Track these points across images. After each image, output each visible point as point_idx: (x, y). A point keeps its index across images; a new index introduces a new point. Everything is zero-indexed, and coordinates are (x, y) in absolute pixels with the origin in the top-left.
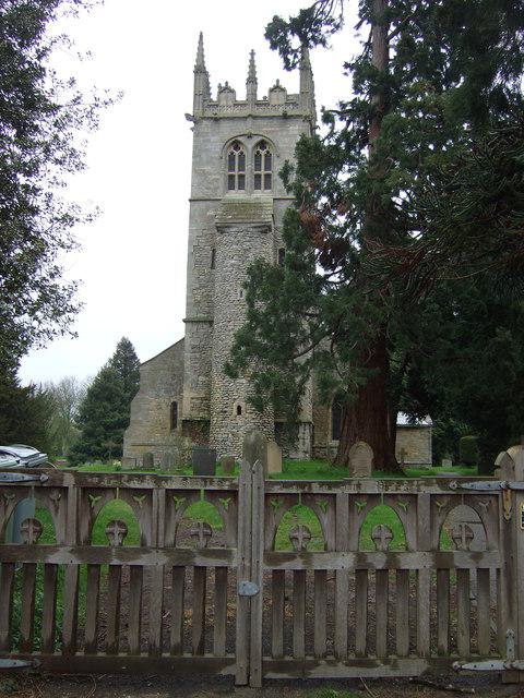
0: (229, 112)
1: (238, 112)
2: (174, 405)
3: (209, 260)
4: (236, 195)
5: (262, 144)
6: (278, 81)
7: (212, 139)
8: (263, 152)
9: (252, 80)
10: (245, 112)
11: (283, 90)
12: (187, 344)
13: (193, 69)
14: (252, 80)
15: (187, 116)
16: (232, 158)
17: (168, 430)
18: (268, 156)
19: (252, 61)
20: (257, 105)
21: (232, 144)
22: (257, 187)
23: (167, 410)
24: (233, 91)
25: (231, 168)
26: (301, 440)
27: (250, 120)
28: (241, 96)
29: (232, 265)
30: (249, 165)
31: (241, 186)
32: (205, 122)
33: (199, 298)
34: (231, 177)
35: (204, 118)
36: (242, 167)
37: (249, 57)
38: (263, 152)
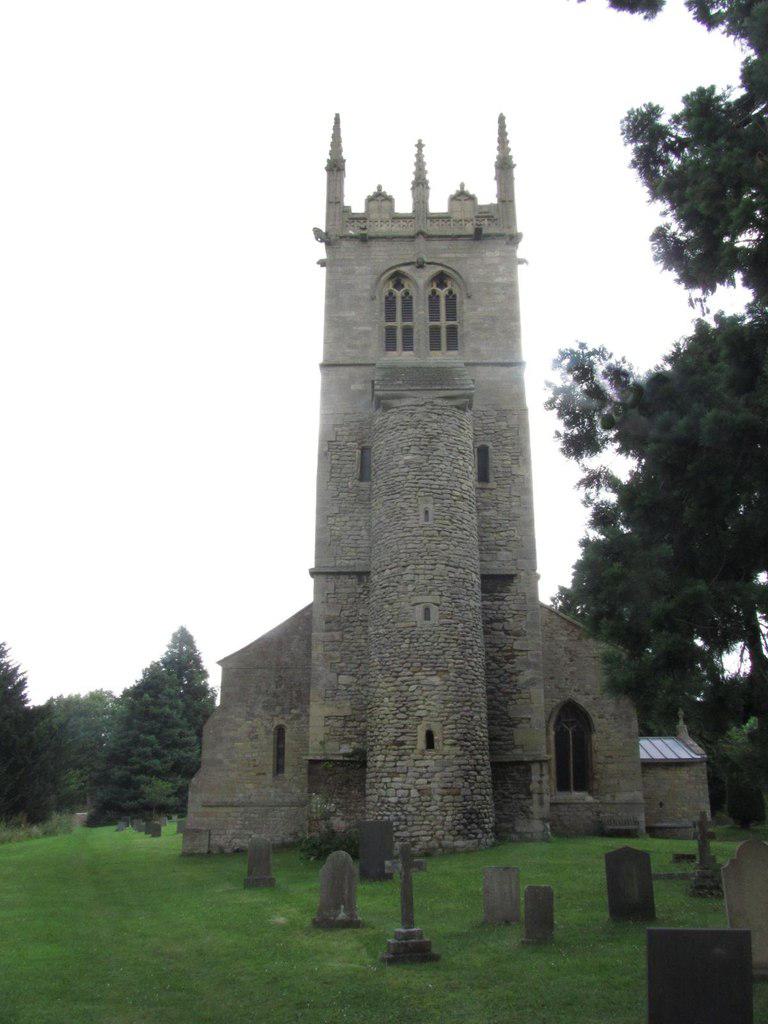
0: (384, 229)
1: (397, 229)
2: (280, 732)
3: (356, 467)
4: (402, 357)
5: (441, 279)
6: (462, 186)
8: (442, 293)
9: (420, 184)
10: (410, 230)
11: (472, 198)
12: (319, 622)
13: (326, 164)
14: (420, 184)
15: (317, 232)
16: (390, 301)
17: (270, 776)
18: (451, 299)
19: (419, 157)
20: (428, 218)
21: (391, 277)
22: (435, 344)
23: (267, 741)
24: (390, 199)
25: (390, 316)
26: (535, 797)
27: (421, 241)
28: (404, 205)
29: (408, 464)
30: (421, 310)
31: (408, 344)
32: (345, 243)
34: (390, 333)
36: (408, 314)
37: (415, 150)
38: (442, 293)
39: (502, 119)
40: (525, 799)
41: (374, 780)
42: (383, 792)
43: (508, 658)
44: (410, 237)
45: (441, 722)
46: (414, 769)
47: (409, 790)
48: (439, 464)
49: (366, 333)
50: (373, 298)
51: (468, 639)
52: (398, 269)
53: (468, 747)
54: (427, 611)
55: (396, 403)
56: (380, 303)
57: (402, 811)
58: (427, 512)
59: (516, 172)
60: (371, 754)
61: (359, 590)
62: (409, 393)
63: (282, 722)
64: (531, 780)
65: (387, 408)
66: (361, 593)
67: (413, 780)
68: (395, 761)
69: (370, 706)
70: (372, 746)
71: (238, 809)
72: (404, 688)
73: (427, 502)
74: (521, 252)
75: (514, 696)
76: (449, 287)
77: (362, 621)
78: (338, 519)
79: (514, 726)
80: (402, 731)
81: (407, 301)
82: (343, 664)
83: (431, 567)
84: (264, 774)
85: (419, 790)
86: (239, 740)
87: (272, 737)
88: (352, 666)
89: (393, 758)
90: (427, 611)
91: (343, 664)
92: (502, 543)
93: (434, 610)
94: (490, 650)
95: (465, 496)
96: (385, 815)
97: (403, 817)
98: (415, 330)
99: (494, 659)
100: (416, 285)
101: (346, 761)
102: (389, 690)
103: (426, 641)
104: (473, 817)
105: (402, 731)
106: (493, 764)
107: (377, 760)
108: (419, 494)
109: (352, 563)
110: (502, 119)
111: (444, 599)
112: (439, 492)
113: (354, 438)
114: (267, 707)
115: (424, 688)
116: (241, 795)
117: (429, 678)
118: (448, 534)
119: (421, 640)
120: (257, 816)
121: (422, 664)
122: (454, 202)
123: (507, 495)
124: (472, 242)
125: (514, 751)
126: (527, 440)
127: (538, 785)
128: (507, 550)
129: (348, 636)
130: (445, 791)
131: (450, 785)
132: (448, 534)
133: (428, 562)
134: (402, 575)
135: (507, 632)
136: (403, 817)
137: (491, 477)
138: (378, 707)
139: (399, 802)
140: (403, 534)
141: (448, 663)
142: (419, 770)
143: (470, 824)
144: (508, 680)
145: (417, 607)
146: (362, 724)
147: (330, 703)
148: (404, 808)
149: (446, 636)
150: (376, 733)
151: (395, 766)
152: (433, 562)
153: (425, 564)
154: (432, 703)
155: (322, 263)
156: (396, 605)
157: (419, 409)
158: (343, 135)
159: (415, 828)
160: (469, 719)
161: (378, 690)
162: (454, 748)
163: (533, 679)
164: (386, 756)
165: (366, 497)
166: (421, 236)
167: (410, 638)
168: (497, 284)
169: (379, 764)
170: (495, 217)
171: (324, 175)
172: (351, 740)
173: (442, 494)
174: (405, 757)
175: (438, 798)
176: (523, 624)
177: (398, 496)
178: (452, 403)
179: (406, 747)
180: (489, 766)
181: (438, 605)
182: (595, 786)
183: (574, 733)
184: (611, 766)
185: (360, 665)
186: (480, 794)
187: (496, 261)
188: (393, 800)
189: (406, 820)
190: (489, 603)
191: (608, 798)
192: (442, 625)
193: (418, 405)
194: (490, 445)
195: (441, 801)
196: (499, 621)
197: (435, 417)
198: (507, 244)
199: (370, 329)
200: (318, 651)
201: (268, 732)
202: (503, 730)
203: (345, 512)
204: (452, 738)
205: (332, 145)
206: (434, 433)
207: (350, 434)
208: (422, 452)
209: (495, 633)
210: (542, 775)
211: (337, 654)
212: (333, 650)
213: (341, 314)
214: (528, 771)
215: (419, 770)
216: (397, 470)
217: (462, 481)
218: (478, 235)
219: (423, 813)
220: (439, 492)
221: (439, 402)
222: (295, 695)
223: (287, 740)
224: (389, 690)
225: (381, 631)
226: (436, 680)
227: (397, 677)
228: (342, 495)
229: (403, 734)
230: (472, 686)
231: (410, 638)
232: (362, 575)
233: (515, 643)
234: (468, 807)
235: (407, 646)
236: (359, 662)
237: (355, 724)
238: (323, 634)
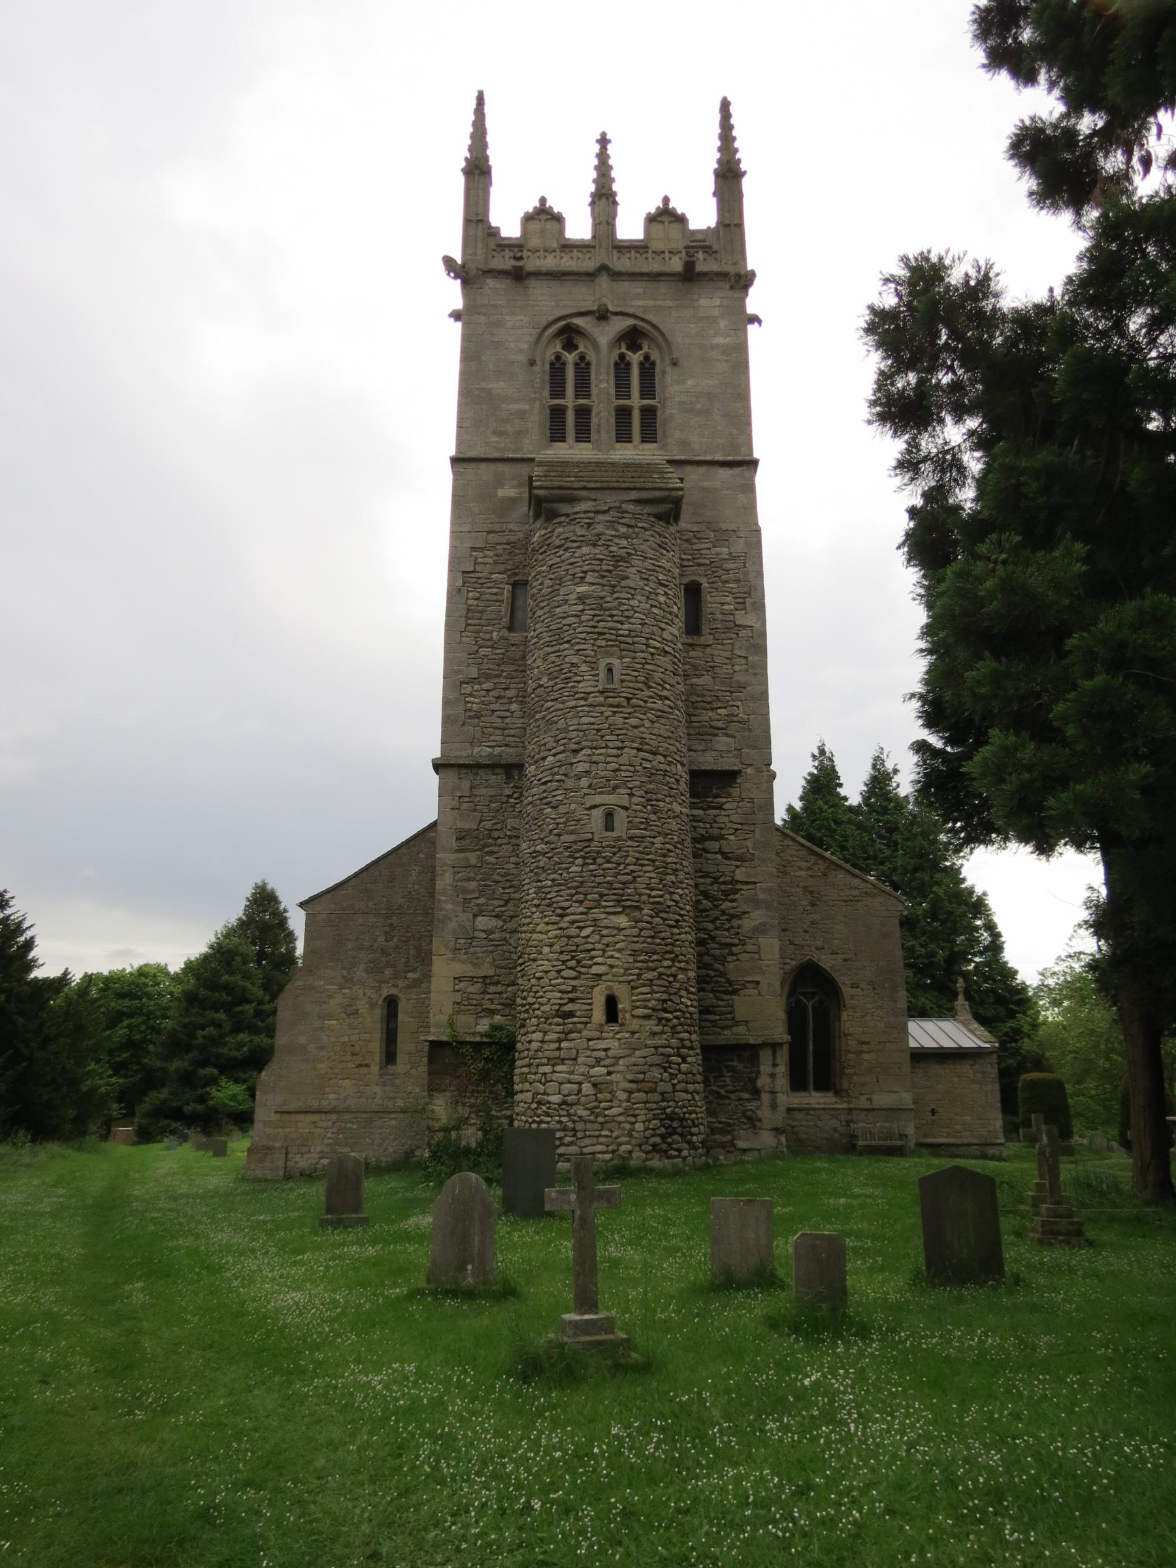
0: (550, 262)
1: (567, 263)
2: (392, 1004)
3: (504, 608)
4: (570, 451)
5: (632, 338)
7: (511, 320)
8: (635, 358)
10: (589, 265)
11: (681, 220)
12: (446, 838)
13: (463, 164)
15: (448, 262)
16: (557, 369)
17: (375, 1068)
18: (648, 369)
20: (615, 247)
22: (623, 435)
23: (373, 1020)
24: (558, 219)
25: (557, 388)
26: (765, 1097)
27: (604, 281)
28: (579, 227)
29: (582, 598)
30: (603, 383)
31: (583, 434)
32: (491, 282)
33: (475, 704)
34: (557, 414)
35: (488, 272)
37: (596, 148)
38: (635, 358)
39: (725, 106)
40: (748, 1100)
41: (526, 1070)
42: (541, 1088)
43: (726, 893)
44: (588, 274)
45: (629, 982)
46: (589, 1053)
47: (580, 1083)
48: (628, 599)
49: (522, 414)
50: (532, 363)
51: (669, 860)
52: (569, 321)
53: (668, 1020)
54: (609, 816)
55: (565, 508)
56: (542, 369)
57: (569, 1115)
58: (610, 670)
59: (746, 183)
60: (523, 1031)
61: (507, 792)
62: (584, 493)
63: (394, 991)
64: (759, 1072)
65: (552, 516)
66: (509, 796)
67: (583, 1069)
68: (559, 1041)
69: (521, 961)
70: (525, 1020)
71: (329, 1116)
72: (573, 931)
73: (611, 655)
74: (754, 303)
75: (735, 950)
76: (645, 349)
77: (510, 837)
78: (476, 687)
79: (735, 992)
80: (570, 995)
81: (583, 367)
82: (482, 901)
83: (615, 752)
84: (367, 1066)
85: (594, 1085)
86: (329, 1017)
87: (378, 1012)
88: (495, 902)
89: (554, 1036)
90: (609, 816)
91: (482, 901)
92: (719, 724)
93: (620, 817)
94: (702, 880)
95: (667, 649)
96: (542, 1122)
97: (570, 1125)
98: (594, 413)
99: (705, 894)
100: (595, 345)
101: (485, 1043)
102: (551, 934)
103: (608, 862)
104: (675, 1124)
105: (570, 995)
106: (703, 1048)
107: (531, 1040)
108: (599, 643)
109: (497, 750)
110: (725, 106)
111: (635, 800)
112: (630, 640)
113: (502, 568)
114: (374, 969)
115: (604, 932)
116: (331, 1096)
117: (611, 917)
118: (642, 703)
119: (599, 860)
120: (355, 1126)
121: (601, 895)
122: (655, 226)
123: (728, 654)
124: (680, 284)
125: (734, 1030)
126: (760, 574)
127: (768, 1080)
128: (728, 735)
129: (491, 859)
130: (634, 1086)
131: (641, 1076)
132: (642, 703)
133: (610, 744)
134: (572, 764)
135: (725, 855)
136: (570, 1125)
137: (705, 629)
138: (534, 960)
139: (564, 1103)
140: (573, 703)
141: (640, 895)
142: (595, 1054)
143: (670, 1135)
144: (727, 926)
145: (594, 812)
146: (510, 989)
147: (465, 957)
148: (572, 1111)
149: (638, 855)
150: (530, 1000)
151: (559, 1049)
152: (620, 745)
153: (607, 747)
154: (618, 955)
155: (456, 316)
156: (562, 809)
157: (600, 517)
158: (489, 124)
159: (587, 1141)
160: (671, 979)
161: (535, 936)
162: (645, 1022)
163: (763, 924)
164: (545, 1033)
165: (519, 654)
166: (604, 273)
167: (584, 858)
168: (718, 346)
169: (534, 1046)
170: (715, 248)
171: (460, 181)
172: (493, 1012)
173: (634, 643)
174: (574, 1035)
175: (623, 1096)
176: (749, 844)
177: (566, 646)
178: (648, 509)
179: (575, 1019)
180: (698, 1051)
181: (626, 808)
182: (845, 1085)
183: (814, 1009)
184: (866, 1056)
185: (507, 902)
186: (686, 1091)
187: (716, 312)
188: (555, 1099)
189: (574, 1129)
190: (701, 812)
191: (863, 1103)
192: (631, 838)
193: (597, 512)
194: (703, 581)
195: (628, 1100)
196: (713, 838)
197: (623, 530)
198: (732, 288)
199: (527, 407)
200: (445, 880)
201: (373, 1006)
202: (718, 999)
203: (488, 677)
204: (645, 1007)
205: (473, 136)
206: (622, 552)
207: (495, 562)
208: (604, 581)
209: (709, 856)
210: (775, 1065)
211: (473, 884)
212: (469, 880)
213: (483, 385)
214: (754, 1060)
215: (595, 1054)
216: (565, 608)
217: (663, 626)
218: (689, 276)
219: (600, 1119)
220: (630, 640)
221: (630, 507)
222: (413, 952)
223: (402, 1017)
224: (551, 934)
225: (539, 848)
226: (622, 921)
227: (562, 916)
228: (483, 651)
229: (571, 1000)
230: (676, 930)
231: (584, 858)
232: (512, 770)
233: (738, 871)
234: (668, 1110)
235: (579, 869)
236: (506, 897)
237: (499, 988)
238: (453, 856)
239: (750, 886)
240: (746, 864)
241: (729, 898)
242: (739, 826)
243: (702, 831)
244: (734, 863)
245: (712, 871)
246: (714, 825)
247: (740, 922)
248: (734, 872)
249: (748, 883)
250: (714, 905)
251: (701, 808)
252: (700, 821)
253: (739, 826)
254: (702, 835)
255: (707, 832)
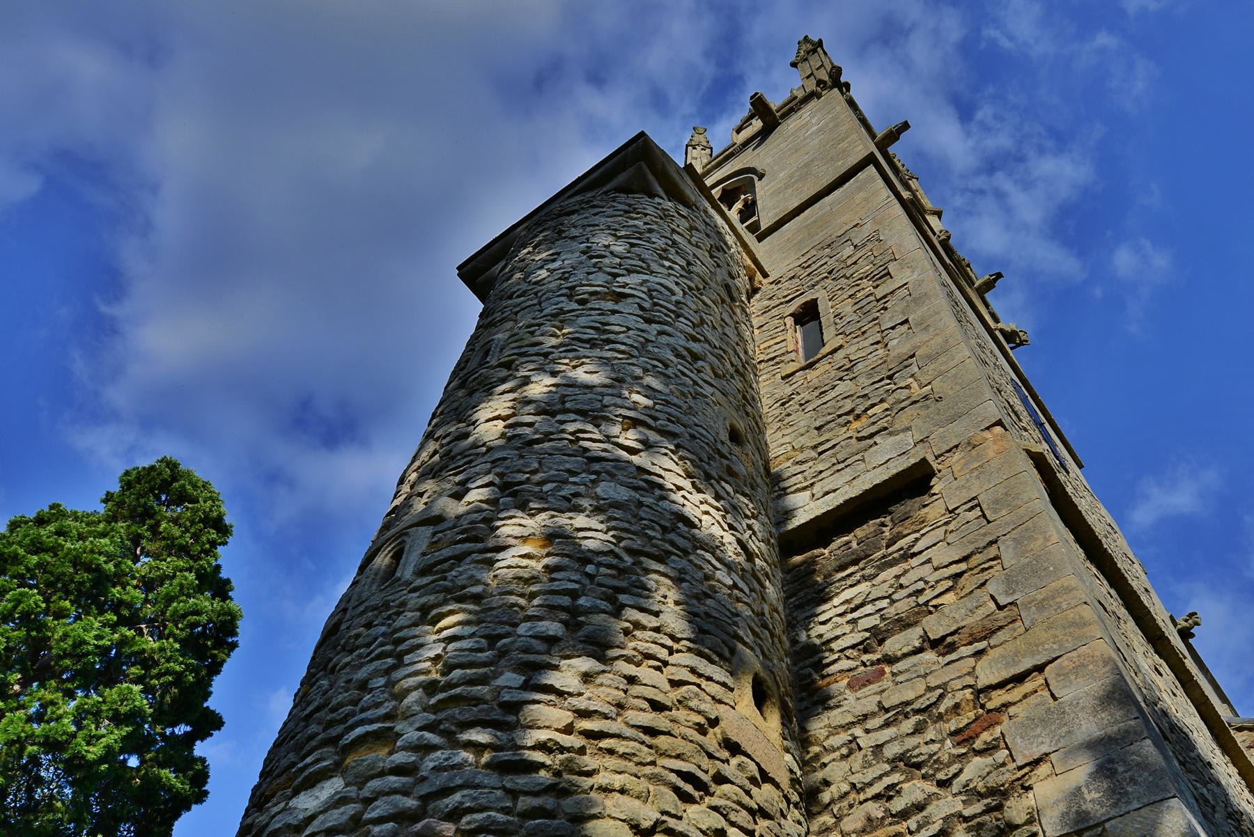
43: (962, 736)
196: (903, 624)
239: (1028, 686)
240: (1000, 636)
241: (978, 745)
242: (963, 566)
243: (874, 621)
244: (965, 651)
245: (910, 695)
246: (895, 597)
247: (1030, 800)
248: (972, 673)
249: (1019, 679)
250: (943, 784)
251: (865, 578)
252: (862, 605)
253: (963, 566)
254: (873, 630)
255: (883, 618)
